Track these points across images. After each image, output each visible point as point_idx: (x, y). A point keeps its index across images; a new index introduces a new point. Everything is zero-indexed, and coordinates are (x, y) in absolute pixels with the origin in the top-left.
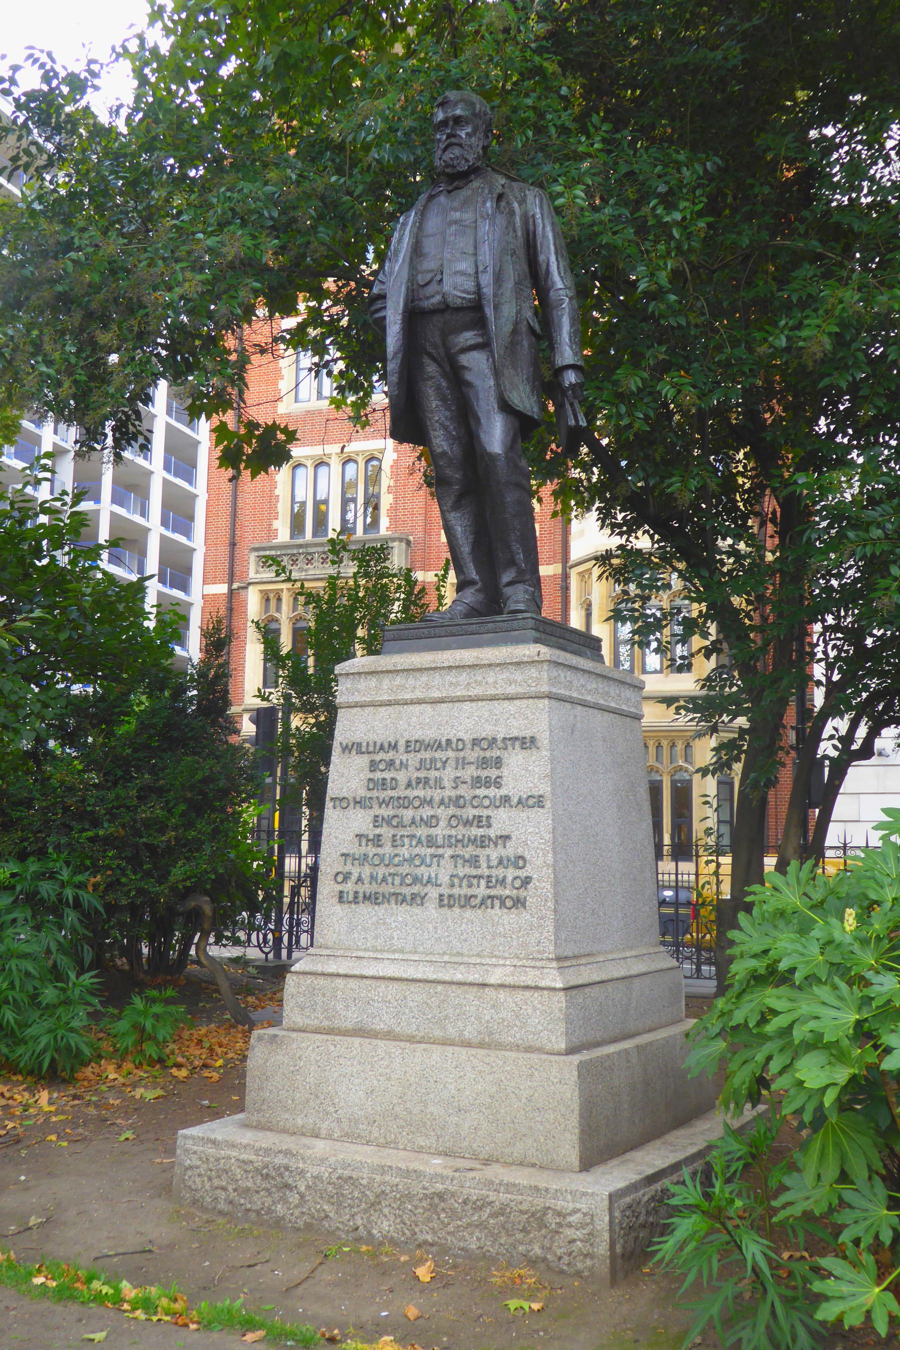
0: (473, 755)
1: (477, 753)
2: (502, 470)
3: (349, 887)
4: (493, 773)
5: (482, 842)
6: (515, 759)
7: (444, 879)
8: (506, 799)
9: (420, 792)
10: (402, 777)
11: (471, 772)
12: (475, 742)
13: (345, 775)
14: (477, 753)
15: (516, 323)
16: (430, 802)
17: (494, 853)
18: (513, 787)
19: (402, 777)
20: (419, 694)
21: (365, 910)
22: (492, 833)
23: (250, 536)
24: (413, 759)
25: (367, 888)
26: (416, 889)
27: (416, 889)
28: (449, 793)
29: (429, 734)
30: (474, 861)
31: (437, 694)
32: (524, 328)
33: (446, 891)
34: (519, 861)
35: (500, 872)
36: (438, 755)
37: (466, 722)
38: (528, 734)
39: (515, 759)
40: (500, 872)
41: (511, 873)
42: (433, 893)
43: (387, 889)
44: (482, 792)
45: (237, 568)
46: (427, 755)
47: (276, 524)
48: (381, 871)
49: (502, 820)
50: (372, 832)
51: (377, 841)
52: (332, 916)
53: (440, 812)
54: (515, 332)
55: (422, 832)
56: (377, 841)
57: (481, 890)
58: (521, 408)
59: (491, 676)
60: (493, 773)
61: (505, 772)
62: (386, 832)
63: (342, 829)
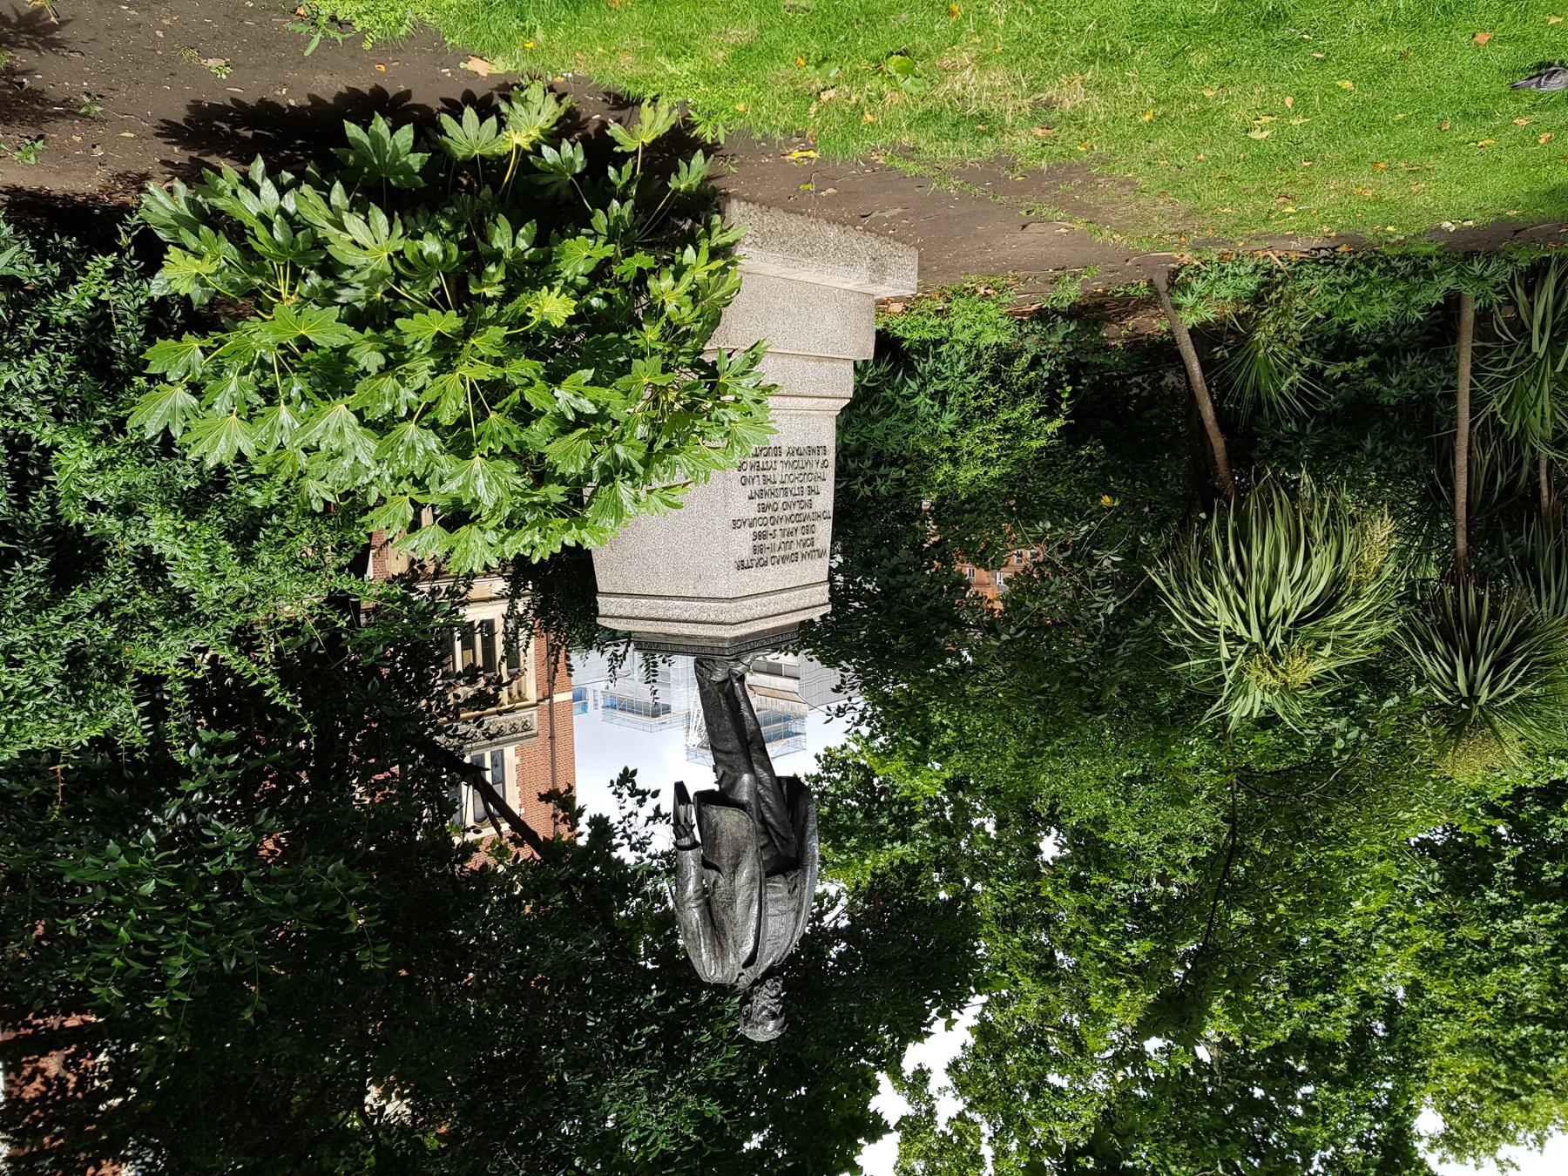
0: (767, 555)
1: (764, 556)
2: (740, 760)
3: (822, 458)
4: (757, 542)
5: (762, 493)
6: (746, 554)
7: (779, 466)
8: (751, 525)
9: (791, 525)
10: (800, 536)
11: (767, 543)
12: (765, 564)
13: (824, 532)
14: (764, 556)
15: (734, 872)
16: (789, 519)
17: (756, 487)
18: (746, 534)
19: (800, 536)
20: (792, 594)
21: (814, 444)
22: (758, 501)
23: (538, 746)
24: (795, 548)
25: (814, 457)
26: (792, 459)
27: (792, 459)
28: (777, 527)
29: (788, 567)
30: (766, 480)
31: (785, 595)
32: (726, 870)
33: (779, 459)
34: (744, 482)
35: (754, 473)
36: (782, 553)
37: (770, 577)
38: (742, 572)
39: (746, 554)
40: (754, 473)
41: (747, 473)
42: (784, 457)
43: (806, 457)
44: (763, 529)
45: (547, 717)
46: (789, 552)
47: (517, 761)
48: (807, 470)
49: (751, 511)
50: (813, 495)
51: (811, 491)
52: (826, 436)
53: (780, 513)
54: (735, 867)
55: (790, 498)
56: (811, 491)
57: (761, 459)
58: (730, 810)
59: (757, 612)
60: (757, 542)
61: (751, 543)
62: (806, 498)
63: (825, 501)
